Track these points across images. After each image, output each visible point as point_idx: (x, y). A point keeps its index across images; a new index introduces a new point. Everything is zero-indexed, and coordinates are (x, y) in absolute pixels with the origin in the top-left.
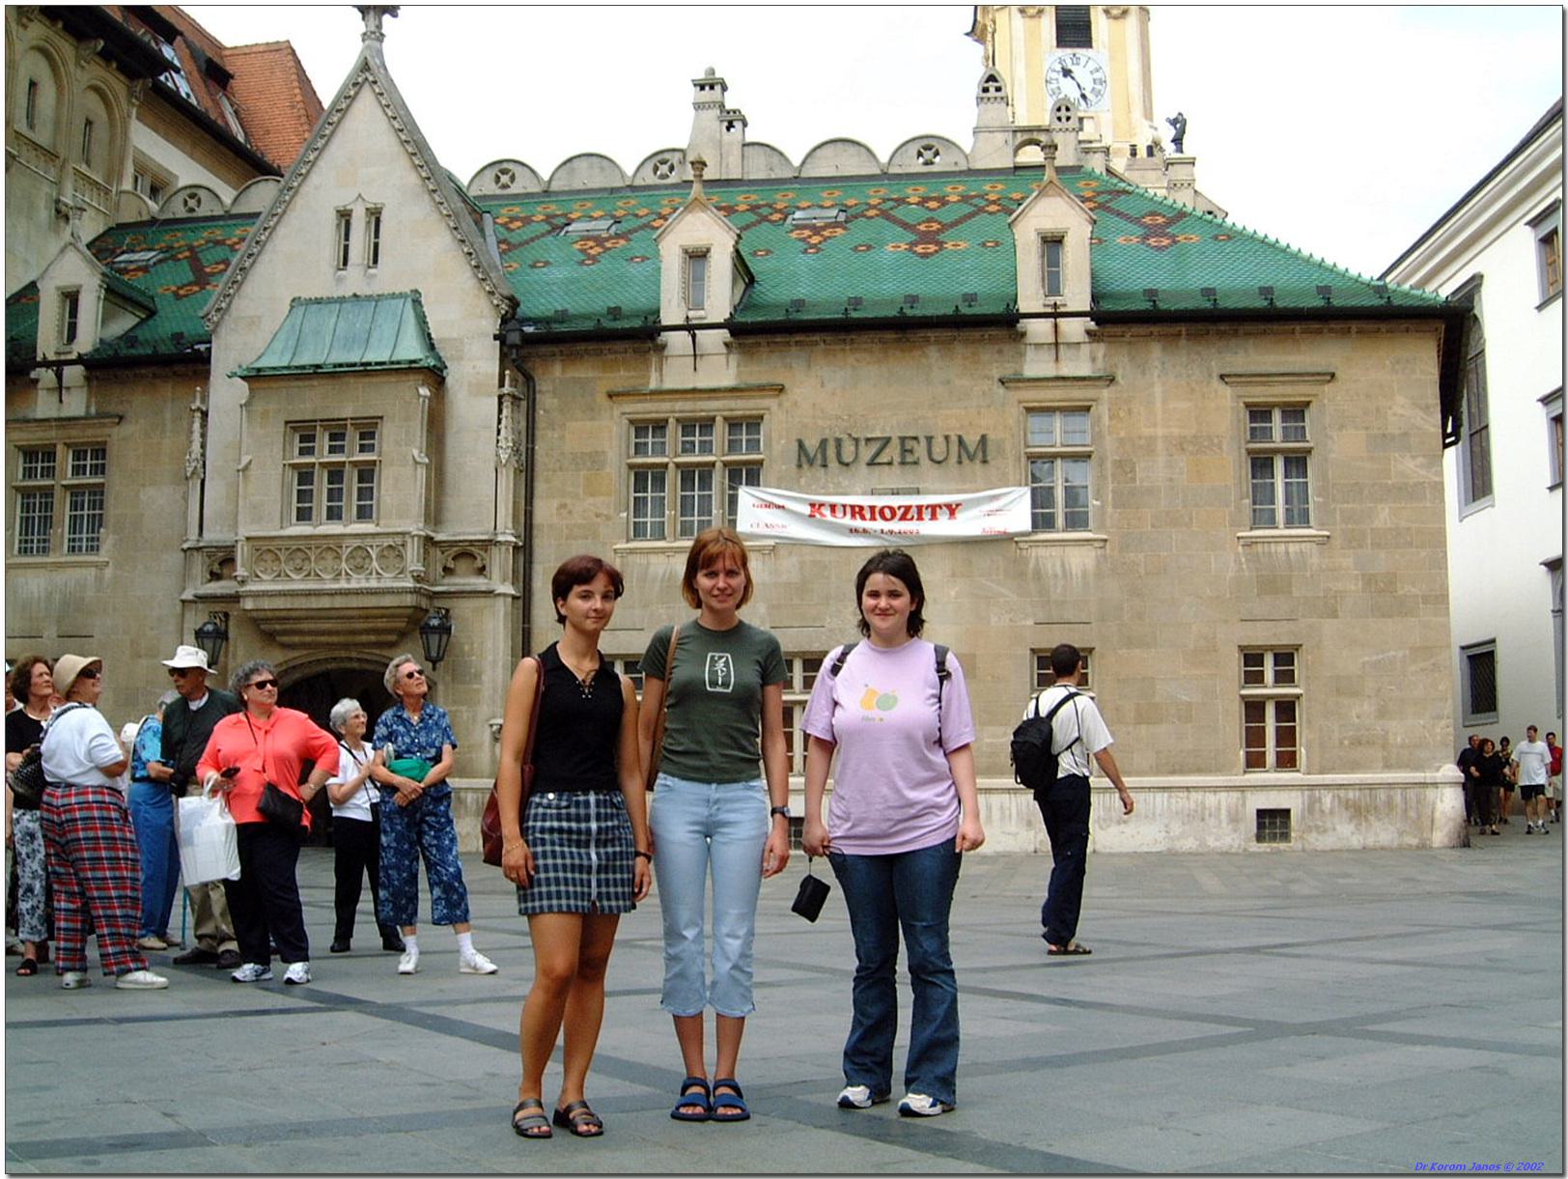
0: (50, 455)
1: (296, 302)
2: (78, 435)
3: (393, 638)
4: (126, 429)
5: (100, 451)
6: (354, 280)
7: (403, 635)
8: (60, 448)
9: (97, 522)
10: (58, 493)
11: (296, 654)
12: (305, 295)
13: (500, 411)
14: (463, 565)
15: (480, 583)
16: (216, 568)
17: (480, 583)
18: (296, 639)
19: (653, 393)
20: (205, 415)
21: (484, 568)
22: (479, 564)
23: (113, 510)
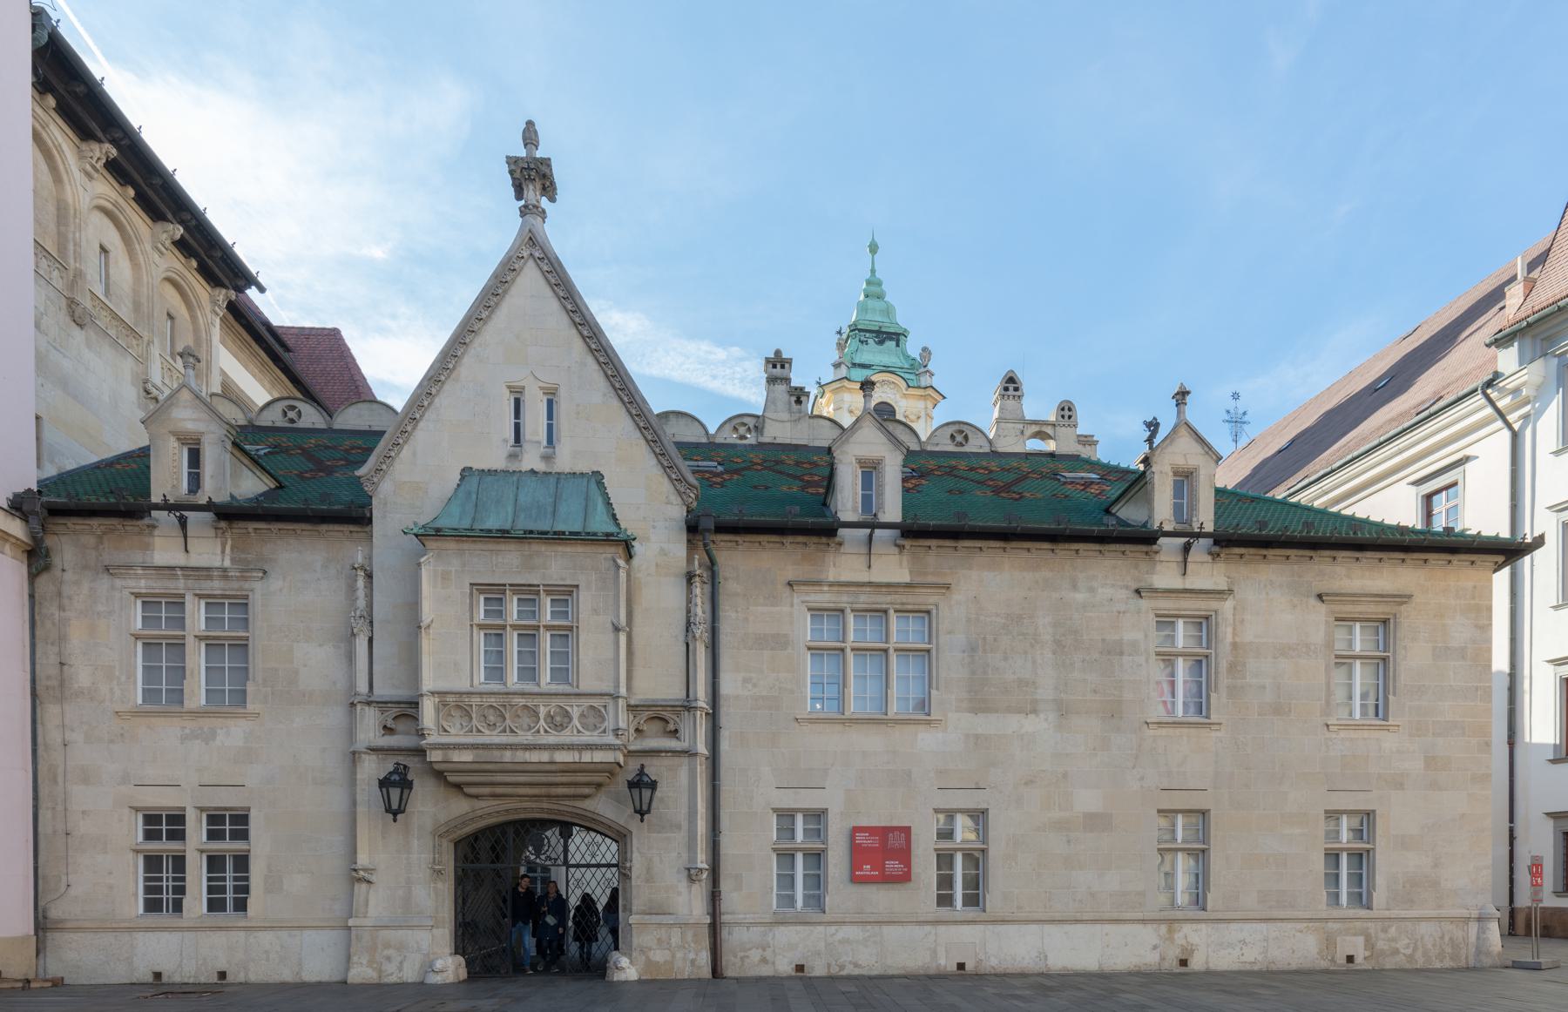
0: (178, 603)
1: (466, 472)
2: (216, 586)
3: (586, 791)
4: (275, 583)
5: (242, 604)
6: (531, 460)
7: (599, 786)
8: (189, 599)
9: (243, 673)
10: (190, 642)
11: (483, 804)
12: (476, 466)
13: (689, 590)
14: (658, 725)
15: (672, 744)
16: (390, 723)
17: (672, 744)
18: (486, 790)
19: (831, 584)
20: (369, 576)
21: (676, 731)
22: (671, 727)
23: (259, 662)
